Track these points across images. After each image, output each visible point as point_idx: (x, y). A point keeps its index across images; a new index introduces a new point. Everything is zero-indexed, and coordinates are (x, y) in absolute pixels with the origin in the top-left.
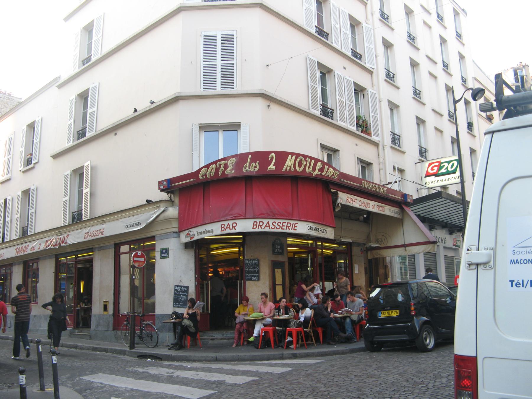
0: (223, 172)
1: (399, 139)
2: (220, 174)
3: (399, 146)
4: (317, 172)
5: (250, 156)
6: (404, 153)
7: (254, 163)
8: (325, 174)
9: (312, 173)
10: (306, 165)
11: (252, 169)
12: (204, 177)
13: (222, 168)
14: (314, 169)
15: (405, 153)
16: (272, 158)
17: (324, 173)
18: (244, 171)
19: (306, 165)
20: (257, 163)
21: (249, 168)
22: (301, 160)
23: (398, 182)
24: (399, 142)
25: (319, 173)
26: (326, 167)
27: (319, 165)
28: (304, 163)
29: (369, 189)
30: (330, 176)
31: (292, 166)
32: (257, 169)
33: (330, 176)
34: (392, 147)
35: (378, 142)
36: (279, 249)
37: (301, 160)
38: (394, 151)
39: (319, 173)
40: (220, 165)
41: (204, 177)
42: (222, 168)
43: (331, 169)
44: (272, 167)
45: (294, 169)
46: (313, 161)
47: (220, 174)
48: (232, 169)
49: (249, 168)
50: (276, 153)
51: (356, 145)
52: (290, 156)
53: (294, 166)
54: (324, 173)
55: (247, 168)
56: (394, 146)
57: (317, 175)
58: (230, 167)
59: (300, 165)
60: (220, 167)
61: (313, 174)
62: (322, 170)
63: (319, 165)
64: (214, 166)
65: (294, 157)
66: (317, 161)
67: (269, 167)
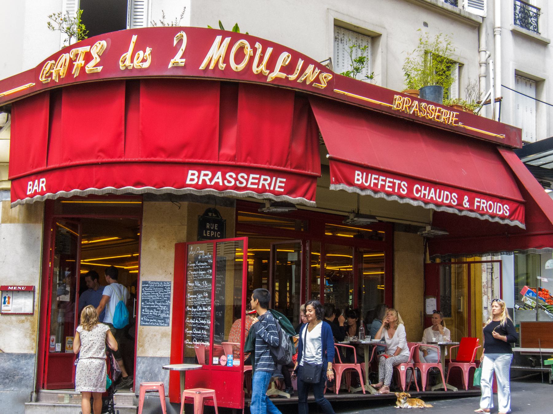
0: (83, 69)
1: (537, 16)
2: (76, 72)
3: (537, 31)
4: (277, 73)
5: (134, 38)
6: (544, 44)
7: (141, 52)
8: (298, 78)
9: (267, 75)
10: (252, 59)
11: (137, 64)
12: (50, 79)
13: (80, 62)
14: (271, 66)
15: (548, 43)
16: (180, 41)
17: (292, 77)
18: (122, 68)
19: (252, 59)
20: (148, 50)
21: (132, 61)
22: (241, 49)
23: (492, 101)
24: (537, 22)
25: (283, 75)
26: (301, 63)
27: (284, 59)
28: (248, 51)
29: (411, 113)
30: (308, 83)
31: (221, 60)
32: (146, 65)
33: (308, 83)
34: (515, 33)
35: (480, 20)
36: (214, 230)
37: (241, 49)
38: (520, 40)
39: (283, 75)
40: (77, 55)
41: (50, 79)
42: (80, 62)
43: (311, 67)
44: (178, 59)
45: (225, 65)
46: (270, 50)
47: (76, 72)
48: (97, 65)
49: (132, 61)
50: (189, 31)
51: (426, 24)
52: (219, 38)
53: (226, 60)
54: (292, 77)
55: (128, 63)
56: (524, 31)
57: (277, 79)
58: (97, 60)
59: (239, 56)
60: (75, 61)
61: (266, 77)
62: (289, 69)
63: (284, 59)
64: (66, 57)
65: (228, 40)
66: (279, 49)
67: (172, 61)
